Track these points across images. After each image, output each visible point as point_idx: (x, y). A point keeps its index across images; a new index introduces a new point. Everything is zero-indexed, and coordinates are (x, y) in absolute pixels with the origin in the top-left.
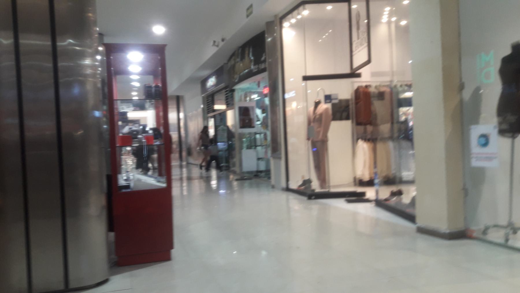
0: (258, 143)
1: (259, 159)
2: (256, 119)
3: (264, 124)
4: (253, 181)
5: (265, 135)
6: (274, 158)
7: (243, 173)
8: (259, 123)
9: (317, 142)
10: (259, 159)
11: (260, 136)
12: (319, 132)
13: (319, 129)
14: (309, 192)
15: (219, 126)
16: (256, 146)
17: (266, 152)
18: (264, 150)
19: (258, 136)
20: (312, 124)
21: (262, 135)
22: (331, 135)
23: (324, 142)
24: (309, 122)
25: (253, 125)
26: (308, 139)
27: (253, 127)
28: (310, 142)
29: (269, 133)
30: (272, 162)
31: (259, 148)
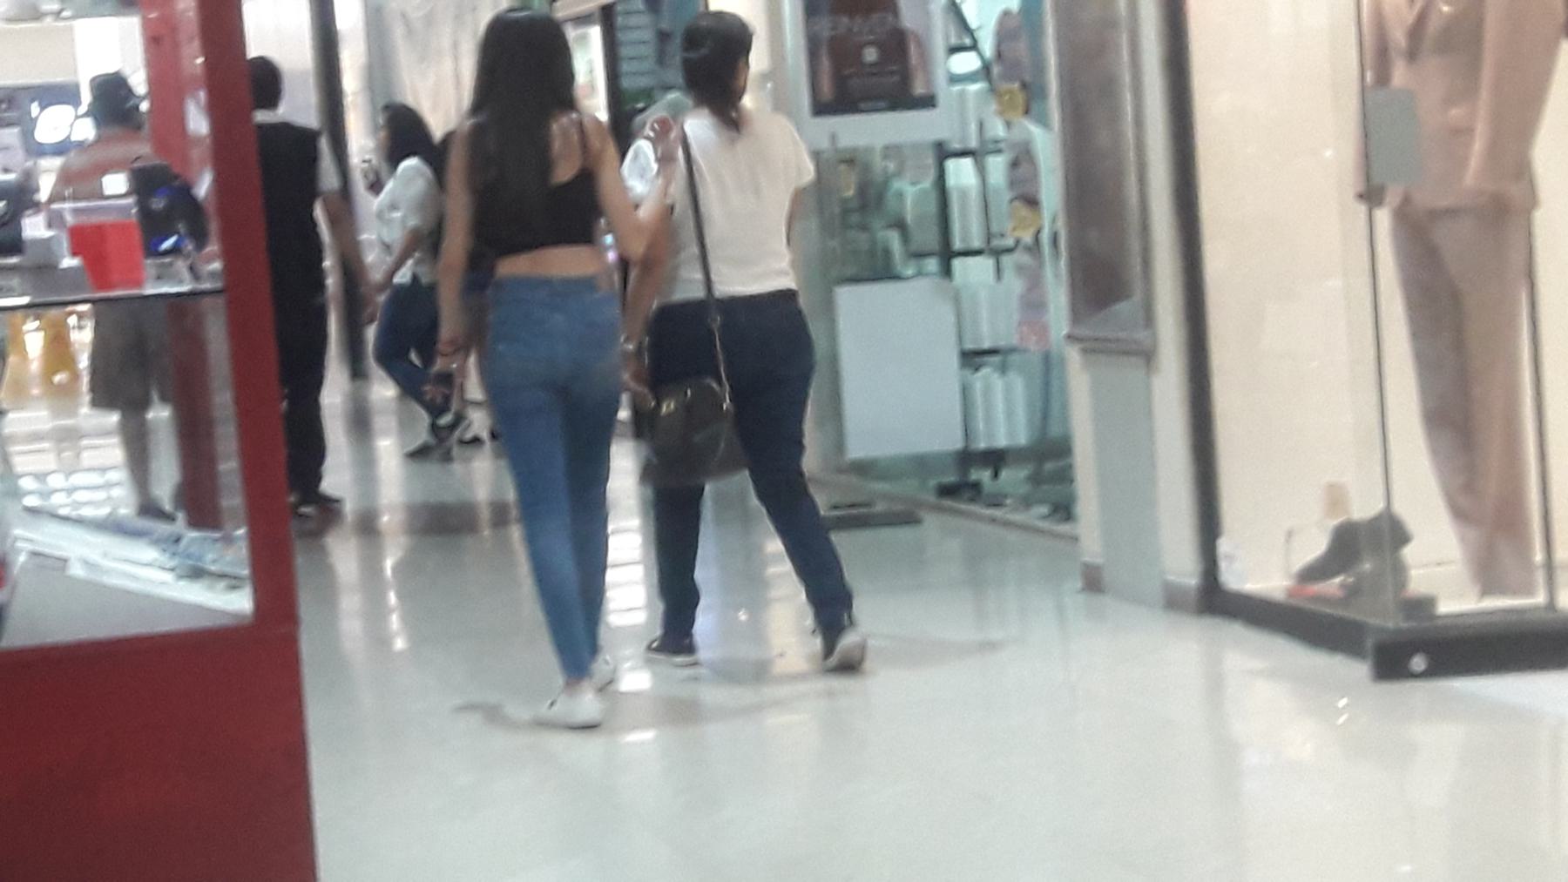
0: (967, 228)
1: (972, 358)
2: (940, 32)
3: (1012, 75)
4: (932, 523)
5: (1022, 160)
6: (1094, 348)
7: (863, 469)
8: (966, 63)
9: (1435, 215)
10: (972, 358)
11: (981, 170)
12: (1469, 131)
13: (1456, 112)
14: (1386, 620)
15: (649, 96)
16: (947, 255)
17: (1033, 304)
18: (1015, 285)
19: (961, 173)
20: (1400, 74)
21: (997, 165)
22: (1549, 154)
23: (1506, 211)
24: (1378, 58)
25: (919, 89)
26: (1371, 195)
27: (928, 102)
28: (1383, 217)
29: (1046, 143)
30: (1080, 383)
31: (973, 272)
